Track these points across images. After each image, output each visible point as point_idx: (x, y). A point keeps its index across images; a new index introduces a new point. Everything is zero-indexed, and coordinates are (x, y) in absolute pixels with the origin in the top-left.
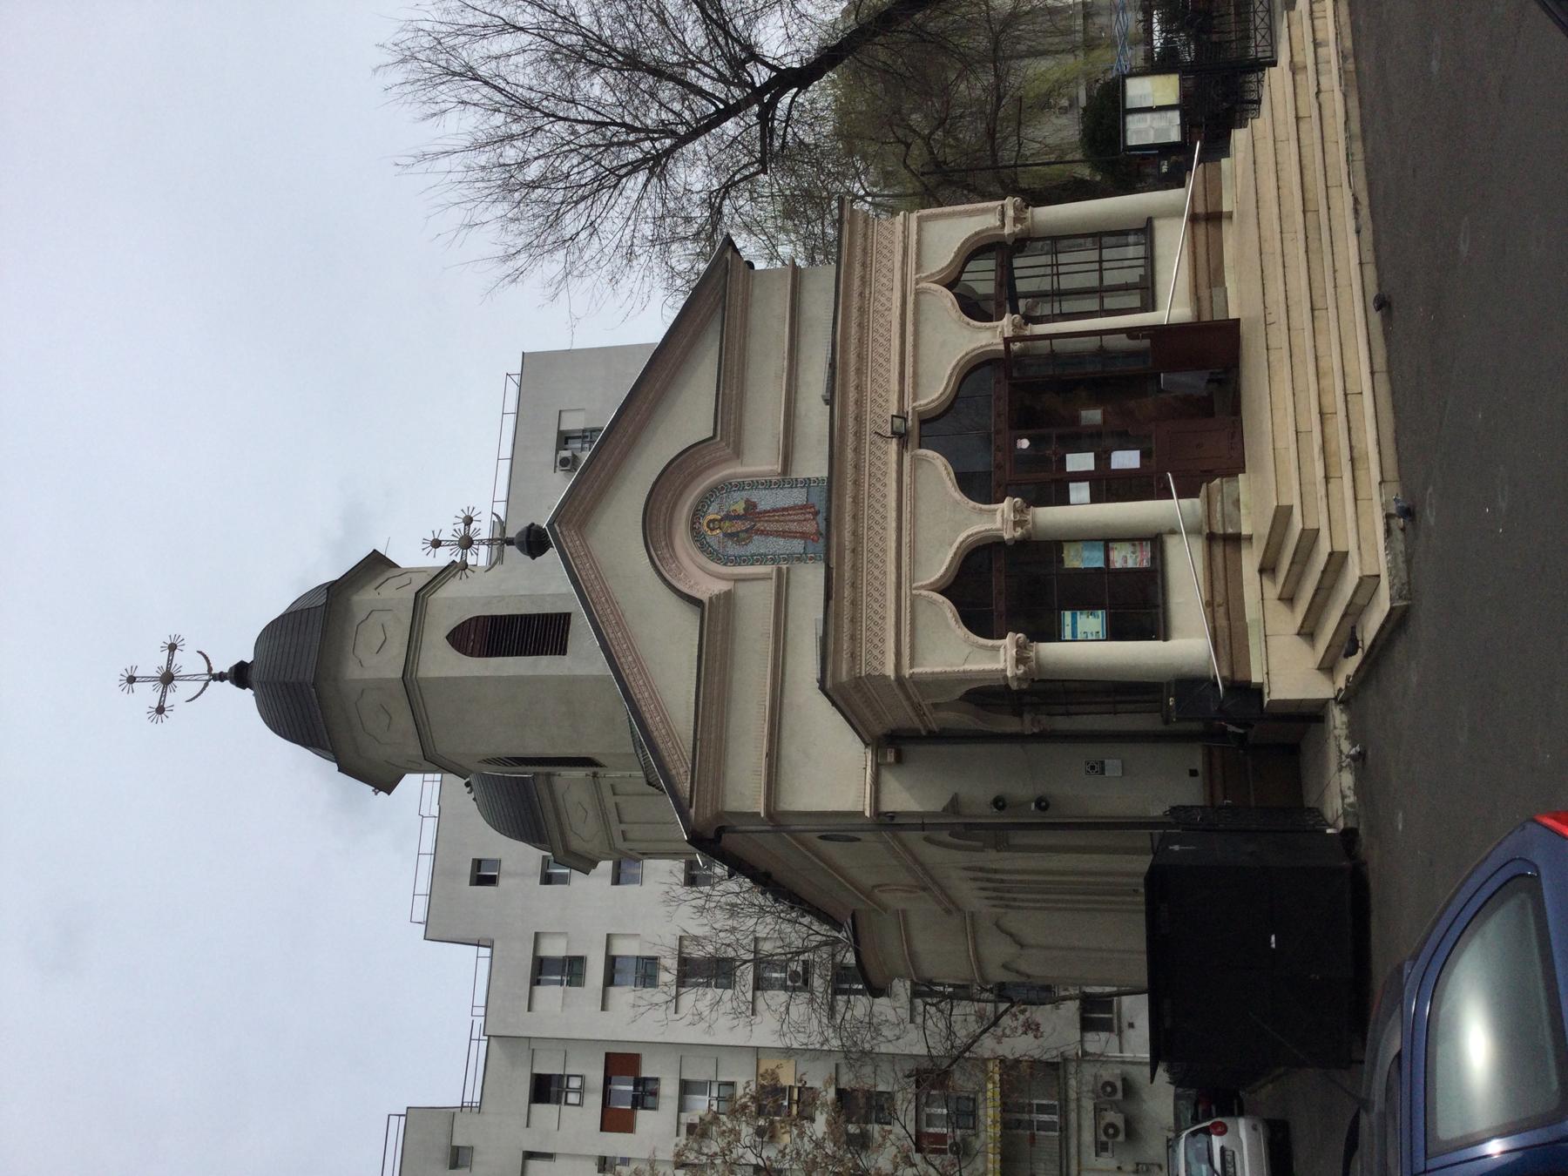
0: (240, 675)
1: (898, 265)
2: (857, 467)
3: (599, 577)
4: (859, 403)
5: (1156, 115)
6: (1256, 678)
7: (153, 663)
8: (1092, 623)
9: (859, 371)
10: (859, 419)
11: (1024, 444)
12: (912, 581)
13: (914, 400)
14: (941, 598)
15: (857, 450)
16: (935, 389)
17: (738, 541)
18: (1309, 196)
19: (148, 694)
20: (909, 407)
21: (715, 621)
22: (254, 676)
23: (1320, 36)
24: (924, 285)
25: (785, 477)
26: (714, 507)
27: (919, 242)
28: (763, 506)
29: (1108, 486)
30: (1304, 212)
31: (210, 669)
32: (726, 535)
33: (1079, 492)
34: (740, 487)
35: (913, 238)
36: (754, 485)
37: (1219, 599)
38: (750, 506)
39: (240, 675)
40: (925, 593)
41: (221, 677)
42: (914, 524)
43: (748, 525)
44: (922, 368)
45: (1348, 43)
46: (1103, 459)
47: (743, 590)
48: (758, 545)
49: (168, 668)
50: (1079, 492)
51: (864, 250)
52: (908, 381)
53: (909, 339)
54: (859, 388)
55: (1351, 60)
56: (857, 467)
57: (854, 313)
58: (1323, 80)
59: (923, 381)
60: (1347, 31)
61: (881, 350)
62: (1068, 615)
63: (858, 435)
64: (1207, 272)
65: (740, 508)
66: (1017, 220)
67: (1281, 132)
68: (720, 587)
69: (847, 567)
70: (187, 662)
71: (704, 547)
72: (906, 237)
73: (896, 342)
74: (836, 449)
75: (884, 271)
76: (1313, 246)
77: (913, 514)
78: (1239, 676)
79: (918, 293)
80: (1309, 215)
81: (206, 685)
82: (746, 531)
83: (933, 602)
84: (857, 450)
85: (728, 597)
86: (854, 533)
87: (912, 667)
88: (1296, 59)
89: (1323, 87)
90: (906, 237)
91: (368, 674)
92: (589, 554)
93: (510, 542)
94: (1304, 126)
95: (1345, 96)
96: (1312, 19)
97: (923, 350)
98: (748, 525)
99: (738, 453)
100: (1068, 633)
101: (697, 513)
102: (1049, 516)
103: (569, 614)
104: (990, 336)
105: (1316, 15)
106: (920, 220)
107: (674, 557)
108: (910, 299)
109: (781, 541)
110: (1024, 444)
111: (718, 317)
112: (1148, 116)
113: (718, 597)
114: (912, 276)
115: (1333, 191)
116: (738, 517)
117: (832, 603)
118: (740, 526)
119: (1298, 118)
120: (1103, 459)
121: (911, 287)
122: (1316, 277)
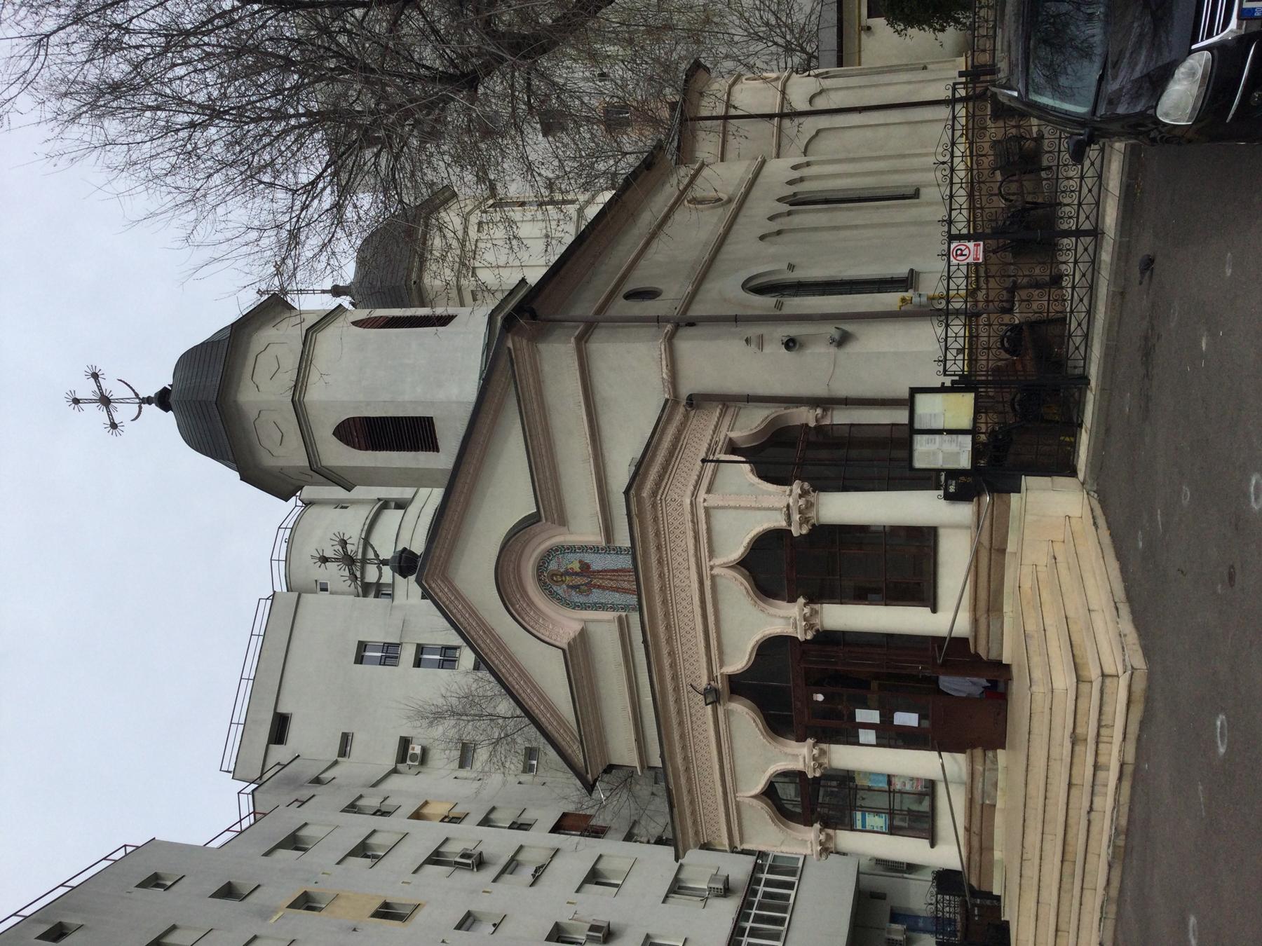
0: (163, 400)
1: (692, 552)
2: (679, 712)
3: (474, 613)
4: (673, 665)
5: (946, 437)
6: (996, 892)
7: (87, 389)
8: (878, 821)
9: (669, 640)
10: (675, 677)
11: (820, 697)
12: (735, 792)
13: (721, 667)
14: (758, 804)
15: (678, 701)
16: (738, 662)
17: (581, 592)
18: (1069, 849)
19: (96, 414)
20: (717, 672)
21: (578, 657)
22: (172, 399)
23: (1102, 760)
24: (715, 571)
25: (609, 547)
26: (553, 566)
27: (709, 530)
28: (594, 567)
29: (891, 737)
30: (1062, 862)
31: (137, 395)
32: (568, 586)
33: (868, 736)
34: (572, 549)
35: (703, 527)
36: (584, 549)
37: (975, 829)
38: (585, 567)
39: (163, 400)
40: (747, 800)
41: (148, 401)
42: (732, 756)
43: (586, 580)
44: (725, 641)
45: (1123, 822)
46: (887, 718)
47: (592, 628)
48: (597, 596)
49: (102, 393)
50: (868, 736)
51: (657, 534)
52: (714, 652)
53: (711, 619)
54: (672, 653)
55: (1123, 837)
56: (679, 712)
57: (656, 587)
58: (1097, 800)
59: (728, 650)
60: (1125, 810)
61: (686, 620)
62: (859, 815)
63: (677, 689)
64: (988, 594)
65: (576, 567)
66: (804, 520)
67: (1055, 753)
68: (576, 627)
69: (683, 781)
70: (115, 390)
71: (552, 595)
72: (695, 522)
73: (699, 620)
74: (660, 708)
75: (679, 550)
76: (1066, 886)
77: (731, 748)
78: (985, 888)
79: (713, 577)
80: (1066, 864)
81: (140, 408)
82: (586, 585)
83: (752, 806)
84: (678, 701)
85: (583, 637)
86: (686, 758)
87: (741, 843)
88: (1079, 730)
89: (1095, 806)
90: (695, 522)
91: (281, 463)
92: (459, 596)
93: (385, 562)
94: (1074, 791)
95: (1110, 866)
96: (1097, 743)
97: (726, 627)
98: (586, 580)
99: (562, 520)
100: (859, 827)
101: (541, 567)
102: (844, 757)
103: (438, 451)
104: (786, 618)
105: (1102, 739)
106: (707, 510)
107: (531, 603)
108: (708, 583)
109: (617, 595)
110: (820, 697)
111: (513, 392)
112: (937, 437)
113: (574, 639)
114: (706, 564)
115: (1087, 893)
116: (576, 574)
117: (676, 810)
118: (578, 580)
119: (1070, 785)
120: (887, 718)
121: (706, 574)
122: (1064, 908)
